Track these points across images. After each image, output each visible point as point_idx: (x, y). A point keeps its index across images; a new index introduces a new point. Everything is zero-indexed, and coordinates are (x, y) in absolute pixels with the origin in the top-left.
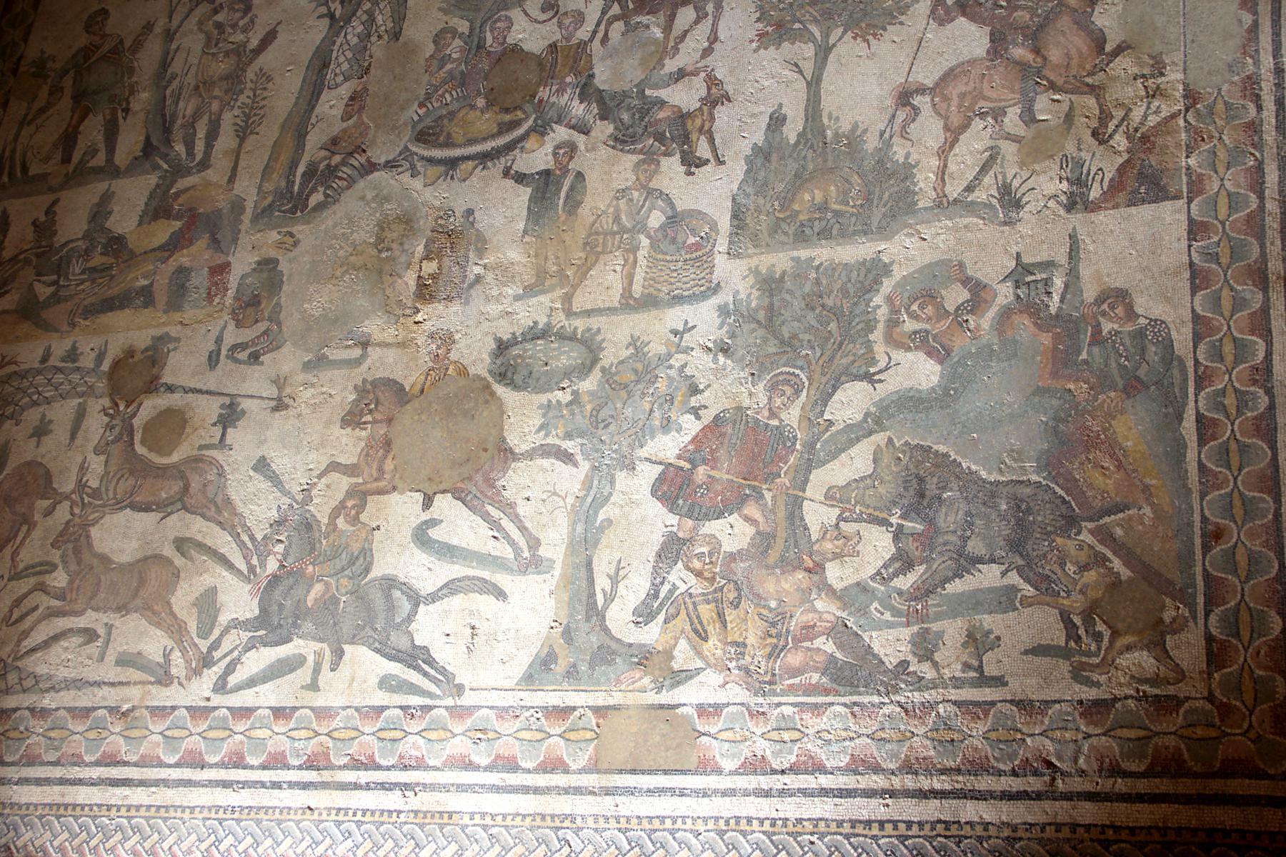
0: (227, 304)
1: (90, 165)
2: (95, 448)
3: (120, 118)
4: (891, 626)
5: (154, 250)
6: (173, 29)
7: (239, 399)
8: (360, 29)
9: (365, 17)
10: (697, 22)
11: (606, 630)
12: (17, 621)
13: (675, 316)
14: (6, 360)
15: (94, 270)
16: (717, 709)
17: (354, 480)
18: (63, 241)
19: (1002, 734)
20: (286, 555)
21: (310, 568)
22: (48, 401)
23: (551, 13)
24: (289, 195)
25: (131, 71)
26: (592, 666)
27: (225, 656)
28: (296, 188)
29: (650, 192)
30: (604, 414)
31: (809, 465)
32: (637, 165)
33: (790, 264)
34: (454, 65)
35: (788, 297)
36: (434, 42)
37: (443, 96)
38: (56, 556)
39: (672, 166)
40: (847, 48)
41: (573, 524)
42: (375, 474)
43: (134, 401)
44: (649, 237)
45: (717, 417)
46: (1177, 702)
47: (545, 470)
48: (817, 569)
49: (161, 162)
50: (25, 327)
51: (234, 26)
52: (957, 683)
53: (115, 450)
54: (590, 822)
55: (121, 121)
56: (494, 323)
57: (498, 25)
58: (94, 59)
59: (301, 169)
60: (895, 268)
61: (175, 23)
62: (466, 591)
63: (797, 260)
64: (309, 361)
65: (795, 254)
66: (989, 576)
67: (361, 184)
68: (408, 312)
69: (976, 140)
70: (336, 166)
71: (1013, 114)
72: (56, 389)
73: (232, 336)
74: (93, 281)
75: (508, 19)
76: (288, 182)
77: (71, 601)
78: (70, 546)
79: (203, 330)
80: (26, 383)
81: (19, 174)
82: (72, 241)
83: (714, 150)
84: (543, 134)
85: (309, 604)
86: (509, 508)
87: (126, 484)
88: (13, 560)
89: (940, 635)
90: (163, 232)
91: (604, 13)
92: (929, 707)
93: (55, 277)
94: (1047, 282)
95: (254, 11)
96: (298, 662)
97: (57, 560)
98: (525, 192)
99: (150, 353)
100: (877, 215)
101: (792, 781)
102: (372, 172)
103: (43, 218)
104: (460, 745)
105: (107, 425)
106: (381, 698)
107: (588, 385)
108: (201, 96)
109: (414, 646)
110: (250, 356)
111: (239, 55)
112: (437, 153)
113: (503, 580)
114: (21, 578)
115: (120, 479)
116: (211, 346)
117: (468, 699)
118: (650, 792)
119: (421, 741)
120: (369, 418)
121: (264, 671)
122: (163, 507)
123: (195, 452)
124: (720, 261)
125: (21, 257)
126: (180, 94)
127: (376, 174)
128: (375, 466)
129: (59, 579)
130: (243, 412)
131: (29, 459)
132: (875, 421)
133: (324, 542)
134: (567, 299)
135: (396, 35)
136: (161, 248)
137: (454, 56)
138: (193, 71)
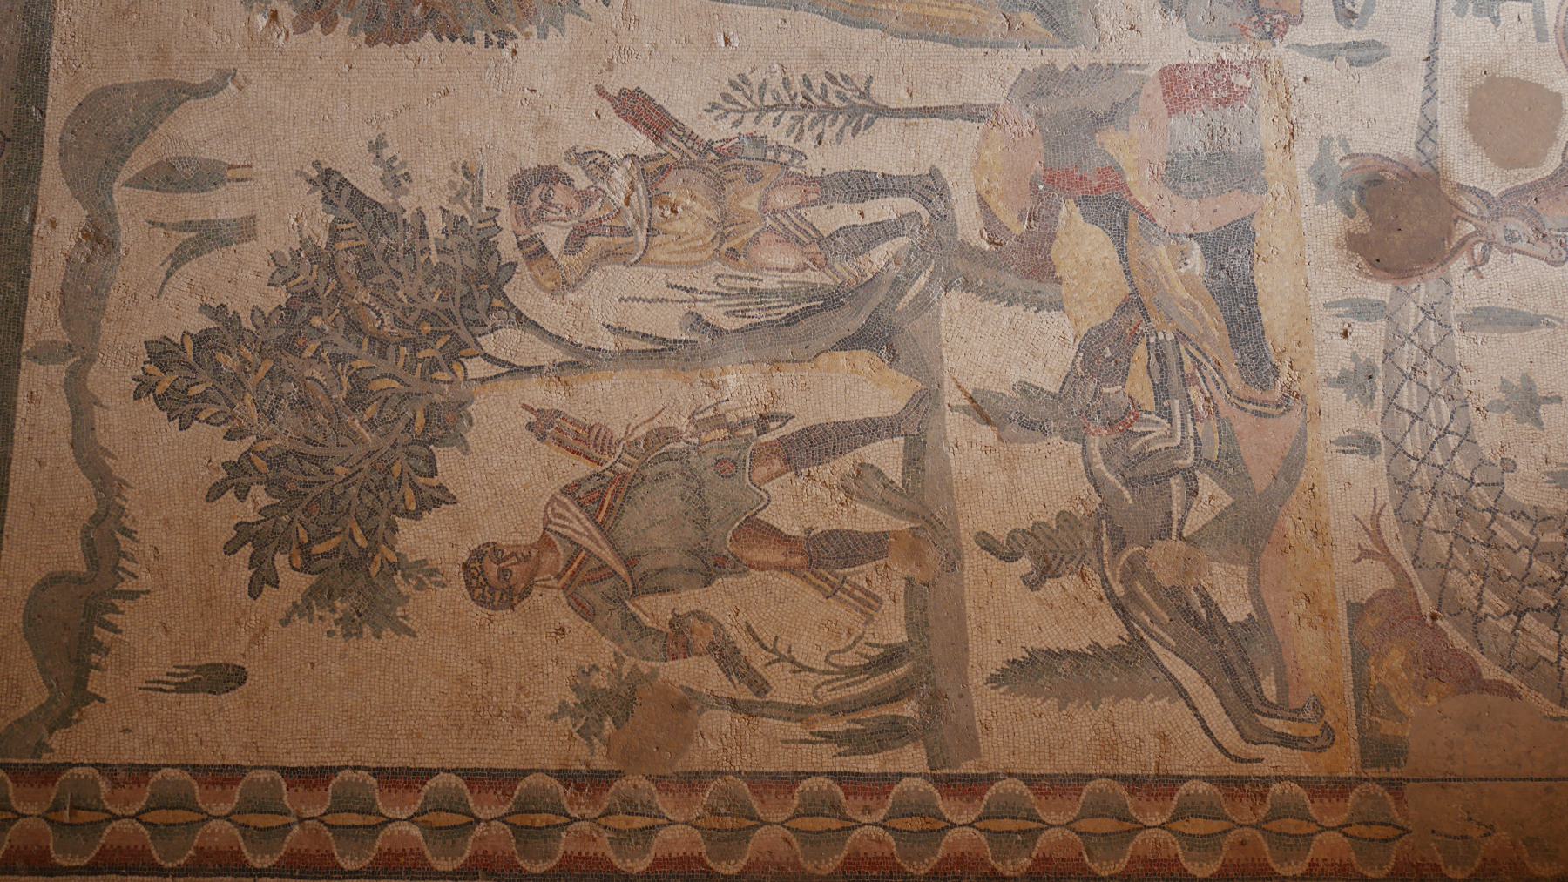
1: (895, 475)
3: (783, 431)
5: (1122, 252)
6: (560, 355)
14: (1369, 544)
15: (1161, 390)
22: (1460, 404)
25: (663, 435)
49: (912, 293)
51: (586, 199)
55: (792, 427)
58: (607, 555)
61: (549, 354)
74: (1186, 381)
80: (1423, 477)
81: (901, 671)
82: (1088, 465)
93: (1175, 482)
103: (1025, 564)
108: (755, 240)
111: (664, 170)
125: (1119, 590)
136: (1119, 235)
138: (680, 277)
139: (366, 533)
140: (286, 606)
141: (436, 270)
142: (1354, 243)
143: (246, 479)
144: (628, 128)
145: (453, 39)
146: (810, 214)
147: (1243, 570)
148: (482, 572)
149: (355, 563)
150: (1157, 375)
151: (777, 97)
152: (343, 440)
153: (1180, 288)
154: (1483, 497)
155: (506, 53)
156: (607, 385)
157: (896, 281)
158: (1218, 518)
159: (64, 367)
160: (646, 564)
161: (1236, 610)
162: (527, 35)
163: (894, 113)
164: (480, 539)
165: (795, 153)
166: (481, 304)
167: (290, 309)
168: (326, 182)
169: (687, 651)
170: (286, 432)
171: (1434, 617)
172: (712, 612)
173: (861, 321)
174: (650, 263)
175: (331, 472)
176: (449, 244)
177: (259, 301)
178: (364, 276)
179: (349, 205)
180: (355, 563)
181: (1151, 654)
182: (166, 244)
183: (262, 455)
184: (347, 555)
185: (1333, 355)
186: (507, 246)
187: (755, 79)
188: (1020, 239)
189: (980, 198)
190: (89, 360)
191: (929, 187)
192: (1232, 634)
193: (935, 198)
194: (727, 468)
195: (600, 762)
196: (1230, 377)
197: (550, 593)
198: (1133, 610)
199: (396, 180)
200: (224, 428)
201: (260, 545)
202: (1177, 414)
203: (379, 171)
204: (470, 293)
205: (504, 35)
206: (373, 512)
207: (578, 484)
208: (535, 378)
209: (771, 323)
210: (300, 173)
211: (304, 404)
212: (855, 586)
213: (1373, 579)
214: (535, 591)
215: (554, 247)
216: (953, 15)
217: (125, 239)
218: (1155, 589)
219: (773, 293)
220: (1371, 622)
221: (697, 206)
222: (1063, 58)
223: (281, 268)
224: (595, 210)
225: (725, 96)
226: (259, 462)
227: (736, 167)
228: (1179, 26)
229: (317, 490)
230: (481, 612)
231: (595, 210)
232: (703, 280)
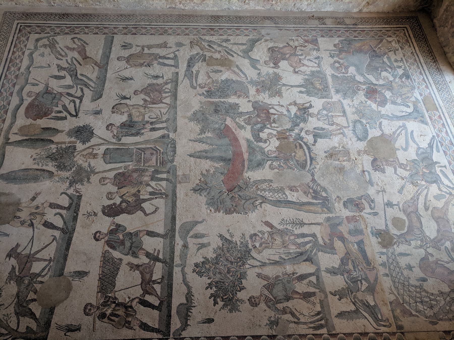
0: (358, 214)
3: (297, 275)
4: (397, 72)
8: (267, 193)
9: (263, 192)
10: (274, 109)
11: (413, 112)
13: (346, 108)
16: (420, 93)
17: (397, 167)
18: (345, 283)
19: (409, 58)
20: (420, 180)
21: (421, 173)
23: (267, 141)
24: (323, 203)
25: (277, 277)
26: (420, 114)
27: (447, 189)
28: (320, 201)
29: (318, 114)
30: (369, 117)
31: (373, 84)
32: (312, 117)
33: (333, 88)
34: (281, 163)
35: (340, 89)
36: (273, 170)
37: (291, 165)
38: (443, 248)
39: (311, 111)
40: (284, 81)
41: (394, 120)
42: (395, 163)
44: (329, 113)
45: (367, 98)
46: (398, 40)
47: (384, 127)
48: (391, 82)
49: (314, 252)
50: (378, 288)
51: (262, 239)
52: (403, 63)
54: (447, 110)
56: (353, 142)
57: (270, 153)
58: (271, 297)
59: (315, 201)
60: (332, 73)
62: (414, 138)
63: (332, 88)
65: (331, 88)
66: (385, 60)
67: (319, 182)
68: (353, 162)
69: (306, 62)
70: (313, 190)
71: (300, 57)
72: (395, 267)
73: (368, 210)
74: (358, 266)
75: (268, 151)
76: (318, 204)
77: (452, 238)
78: (438, 244)
79: (367, 220)
80: (397, 280)
81: (321, 315)
82: (345, 280)
83: (308, 103)
84: (303, 138)
85: (429, 172)
86: (394, 133)
87: (417, 232)
88: (449, 263)
89: (397, 65)
90: (338, 244)
91: (269, 128)
92: (409, 66)
93: (359, 282)
94: (333, 54)
95: (256, 232)
96: (441, 171)
98: (319, 140)
99: (378, 236)
100: (321, 76)
101: (427, 82)
102: (315, 179)
103: (338, 297)
104: (444, 134)
105: (402, 244)
106: (442, 152)
107: (364, 121)
108: (288, 244)
109: (429, 147)
110: (373, 203)
111: (273, 233)
112: (309, 162)
113: (409, 132)
115: (416, 234)
117: (435, 135)
118: (438, 101)
119: (446, 142)
120: (382, 167)
121: (447, 179)
122: (419, 217)
123: (402, 212)
124: (333, 100)
125: (353, 300)
126: (287, 253)
127: (315, 178)
128: (393, 163)
130: (388, 201)
131: (419, 269)
132: (362, 75)
133: (414, 171)
134: (345, 127)
135: (271, 181)
136: (344, 242)
137: (278, 163)
138: (277, 251)
139: (232, 295)
140: (220, 307)
141: (239, 250)
142: (379, 243)
143: (212, 286)
144: (267, 227)
145: (238, 213)
146: (296, 240)
147: (372, 296)
148: (251, 301)
149: (231, 300)
150: (353, 265)
151: (289, 222)
152: (227, 279)
153: (354, 250)
154: (406, 283)
155: (247, 216)
156: (268, 268)
157: (311, 251)
158: (366, 288)
159: (181, 268)
160: (278, 298)
161: (372, 303)
162: (250, 213)
163: (306, 224)
164: (250, 295)
165: (293, 231)
166: (247, 256)
167: (217, 257)
168: (221, 236)
169: (286, 313)
170: (218, 277)
171: (403, 304)
172: (289, 306)
173: (306, 257)
174: (273, 248)
175: (225, 284)
176: (241, 246)
177: (212, 256)
178: (228, 252)
179: (225, 240)
180: (231, 300)
181: (360, 311)
182: (196, 247)
183: (214, 282)
184: (229, 298)
185: (380, 261)
187: (285, 219)
188: (329, 243)
189: (322, 237)
190: (185, 266)
192: (372, 307)
193: (315, 237)
194: (289, 282)
195: (274, 334)
196: (364, 265)
197: (263, 304)
198: (356, 303)
199: (232, 236)
200: (208, 277)
201: (215, 297)
202: (357, 271)
203: (229, 234)
204: (245, 254)
205: (246, 213)
206: (233, 291)
207: (265, 285)
208: (257, 268)
209: (293, 258)
210: (216, 235)
211: (220, 273)
212: (311, 301)
213: (392, 298)
214: (260, 304)
215: (258, 247)
216: (313, 209)
217: (189, 246)
218: (359, 300)
219: (292, 253)
220: (394, 305)
221: (279, 239)
223: (215, 251)
224: (263, 240)
225: (281, 222)
226: (214, 283)
227: (284, 233)
229: (223, 287)
230: (252, 308)
231: (263, 240)
232: (281, 251)
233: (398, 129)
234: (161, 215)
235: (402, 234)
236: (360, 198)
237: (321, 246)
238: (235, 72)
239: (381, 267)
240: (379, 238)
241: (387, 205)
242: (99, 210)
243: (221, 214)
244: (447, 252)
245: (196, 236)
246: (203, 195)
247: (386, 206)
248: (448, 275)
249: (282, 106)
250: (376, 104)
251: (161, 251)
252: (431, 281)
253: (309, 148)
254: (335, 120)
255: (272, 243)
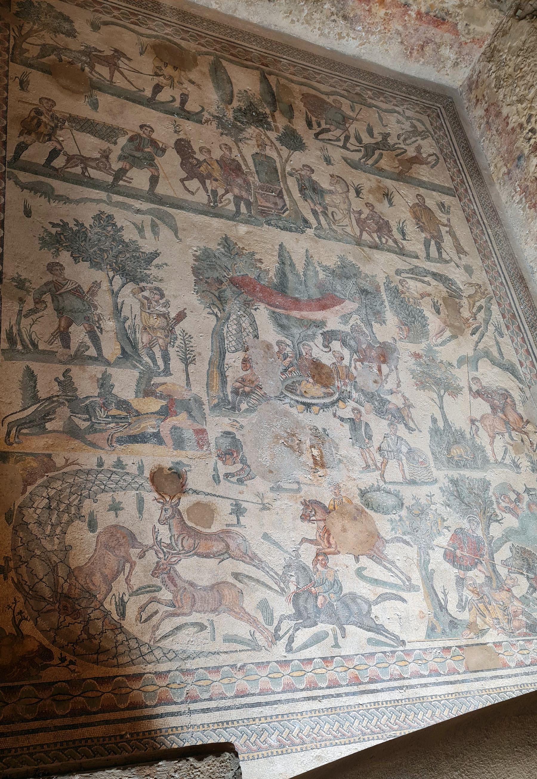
2: (159, 520)
7: (240, 502)
12: (146, 621)
29: (398, 437)
38: (158, 582)
43: (175, 496)
53: (174, 522)
64: (273, 487)
87: (188, 542)
88: (127, 583)
97: (160, 584)
105: (162, 508)
108: (149, 334)
111: (166, 319)
114: (138, 595)
115: (182, 540)
116: (211, 472)
123: (225, 528)
126: (135, 330)
129: (166, 595)
134: (382, 476)
138: (138, 318)
146: (157, 346)
153: (144, 425)
163: (187, 368)
167: (124, 242)
182: (139, 223)
186: (142, 284)
187: (192, 340)
191: (167, 372)
222: (206, 407)
224: (154, 303)
225: (187, 334)
228: (219, 435)
232: (138, 321)
233: (402, 573)
234: (181, 194)
235: (180, 513)
236: (243, 461)
237: (150, 379)
238: (443, 331)
239: (116, 460)
240: (170, 472)
241: (236, 505)
242: (182, 136)
243: (191, 261)
244: (149, 587)
245: (154, 226)
246: (219, 247)
247: (234, 503)
248: (102, 574)
249: (399, 385)
250: (448, 545)
251: (131, 185)
252: (91, 537)
253: (325, 406)
254: (393, 464)
255: (150, 314)
